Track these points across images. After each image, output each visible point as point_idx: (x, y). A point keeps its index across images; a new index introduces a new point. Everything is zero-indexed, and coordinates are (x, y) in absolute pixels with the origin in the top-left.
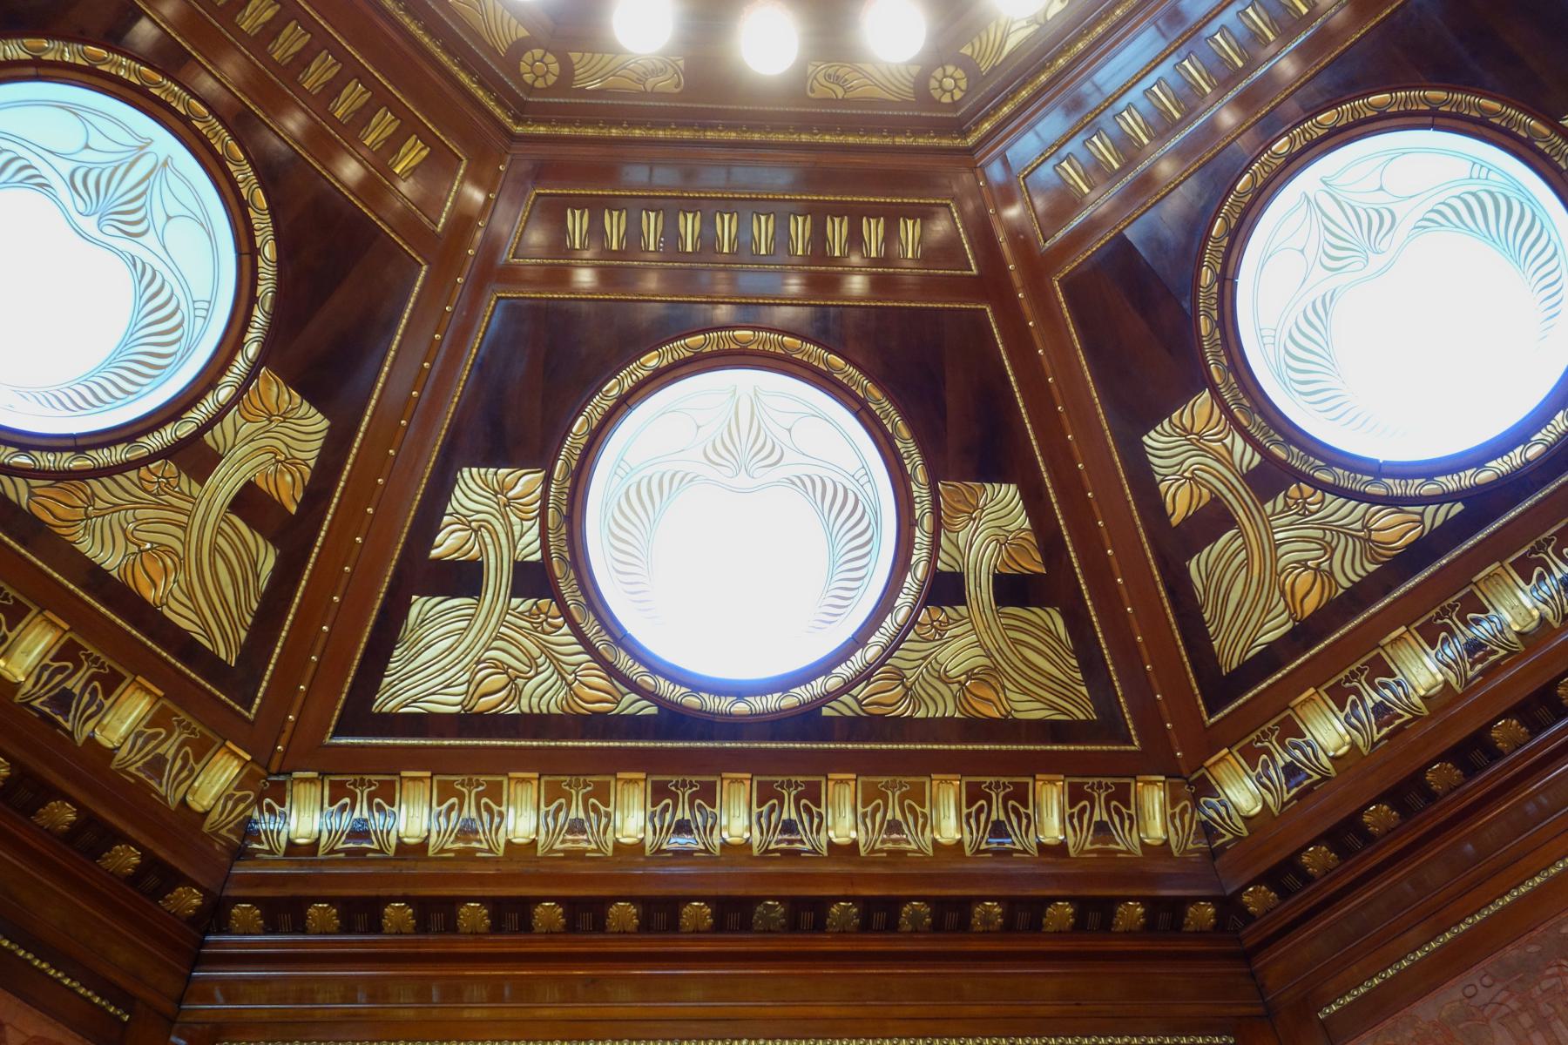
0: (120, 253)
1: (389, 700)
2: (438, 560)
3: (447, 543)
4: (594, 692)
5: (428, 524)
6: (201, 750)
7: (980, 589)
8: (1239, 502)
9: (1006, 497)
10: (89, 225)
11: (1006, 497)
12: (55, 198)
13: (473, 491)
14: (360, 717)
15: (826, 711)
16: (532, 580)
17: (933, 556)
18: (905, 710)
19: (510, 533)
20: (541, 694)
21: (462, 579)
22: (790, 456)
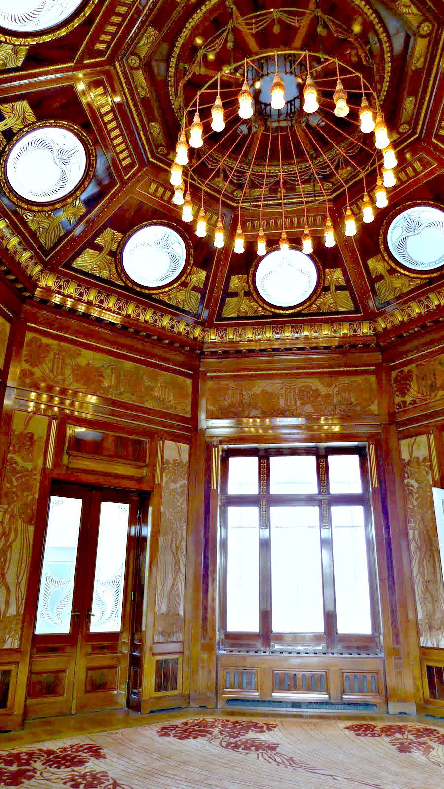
0: (60, 167)
1: (75, 265)
2: (95, 243)
3: (99, 241)
4: (114, 278)
5: (97, 235)
6: (36, 264)
7: (191, 286)
8: (241, 294)
9: (204, 274)
10: (57, 161)
11: (204, 274)
12: (53, 154)
13: (109, 233)
14: (68, 266)
15: (153, 296)
16: (112, 254)
17: (186, 278)
18: (166, 301)
19: (112, 244)
20: (105, 274)
21: (99, 249)
22: (170, 248)
